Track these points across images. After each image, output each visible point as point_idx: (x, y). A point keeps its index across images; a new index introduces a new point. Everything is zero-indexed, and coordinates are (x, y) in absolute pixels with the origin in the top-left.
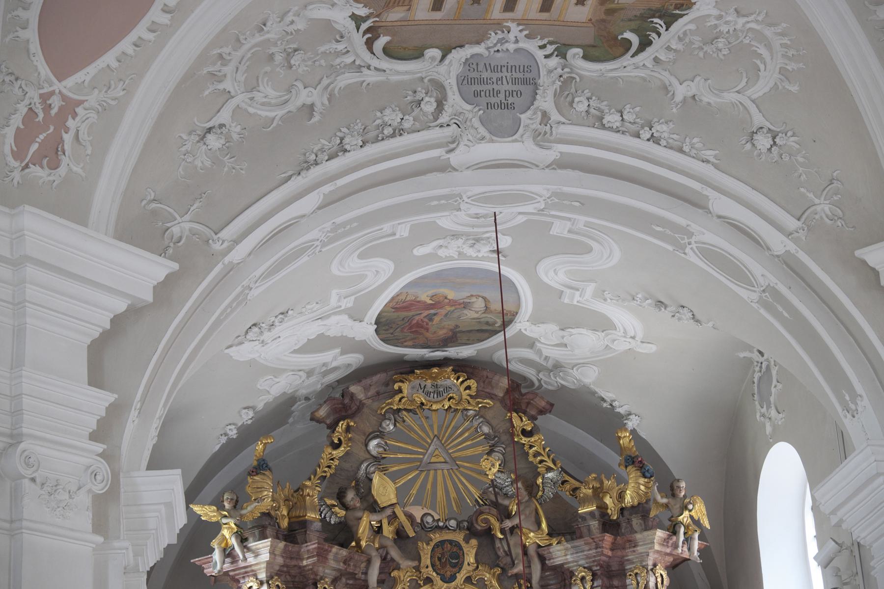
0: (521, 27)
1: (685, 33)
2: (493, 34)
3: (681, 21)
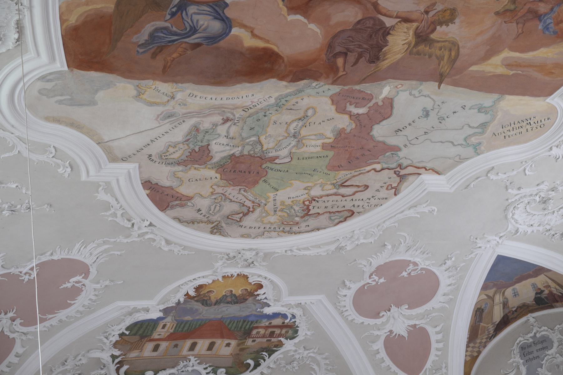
0: (196, 359)
1: (277, 360)
2: (182, 363)
3: (276, 353)
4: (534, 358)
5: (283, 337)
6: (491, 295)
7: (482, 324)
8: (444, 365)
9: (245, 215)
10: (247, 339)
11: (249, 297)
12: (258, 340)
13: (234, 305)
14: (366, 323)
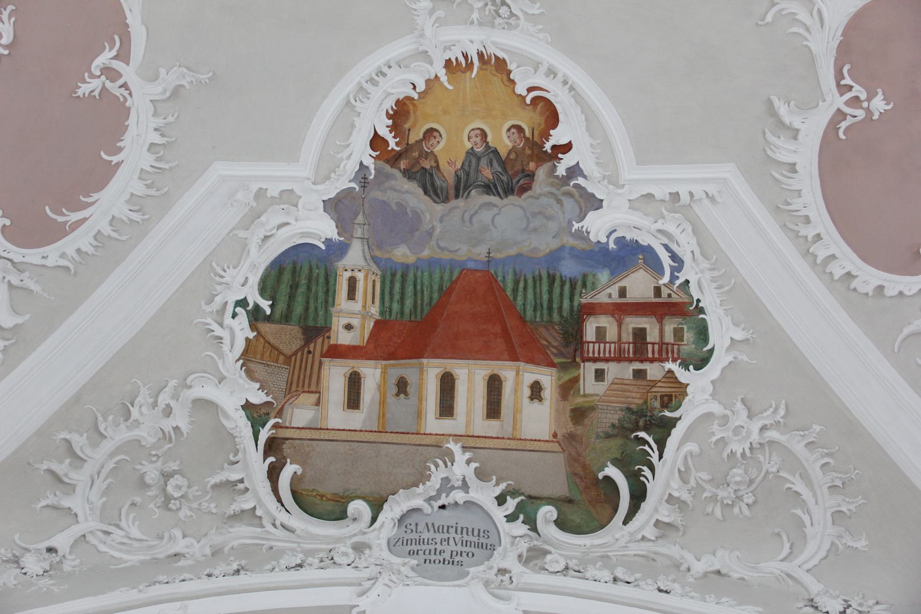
0: (468, 455)
3: (676, 434)
5: (674, 360)
10: (578, 366)
11: (537, 167)
12: (613, 370)
13: (506, 201)
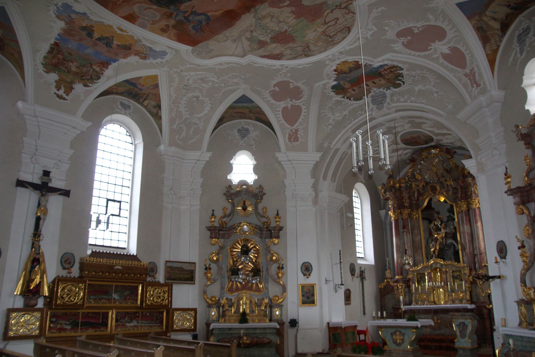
4: (523, 41)
6: (478, 19)
7: (488, 33)
8: (474, 61)
9: (308, 48)
14: (427, 54)
